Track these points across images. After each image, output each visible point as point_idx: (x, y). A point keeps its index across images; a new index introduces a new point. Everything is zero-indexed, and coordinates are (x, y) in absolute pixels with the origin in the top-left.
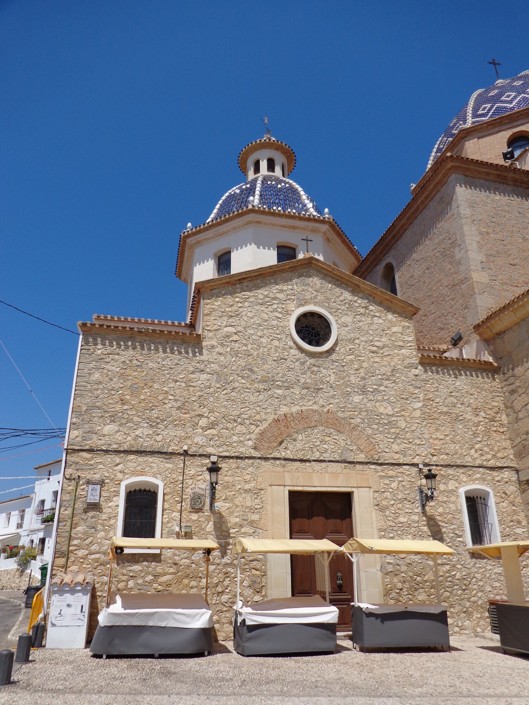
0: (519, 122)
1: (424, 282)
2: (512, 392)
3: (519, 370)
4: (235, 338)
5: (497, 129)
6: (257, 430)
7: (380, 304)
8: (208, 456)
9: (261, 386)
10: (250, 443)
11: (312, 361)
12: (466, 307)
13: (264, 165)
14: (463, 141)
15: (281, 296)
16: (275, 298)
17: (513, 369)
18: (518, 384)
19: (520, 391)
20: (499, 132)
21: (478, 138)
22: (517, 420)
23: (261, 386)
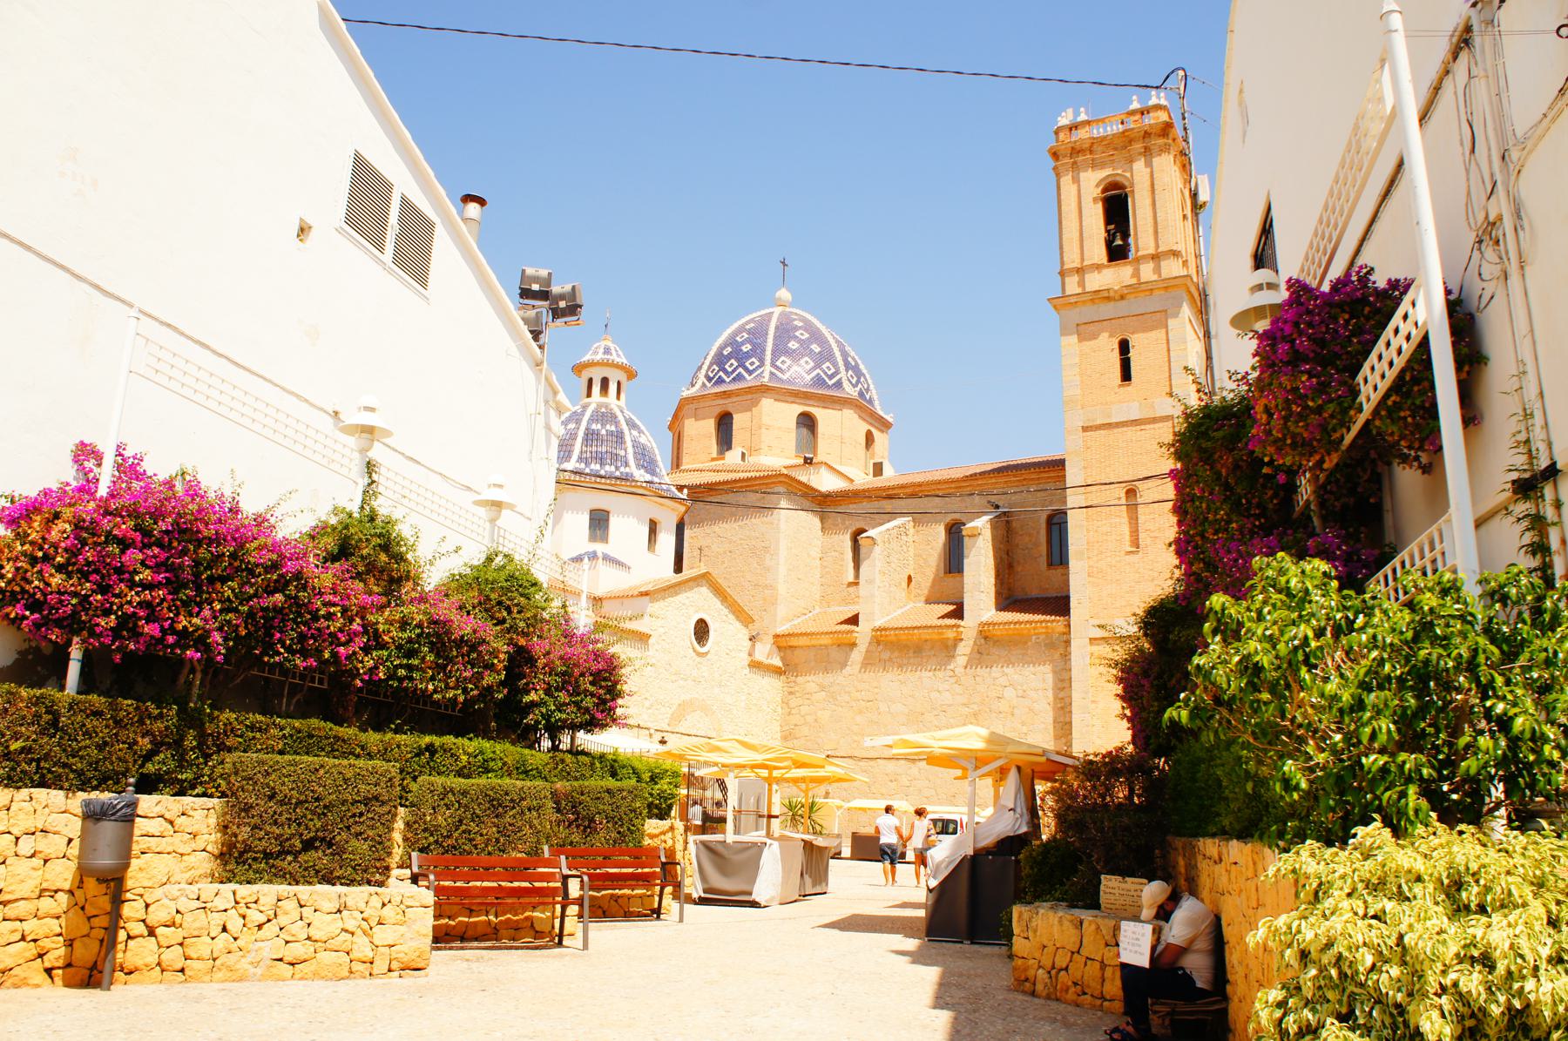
0: (811, 402)
1: (723, 562)
2: (791, 693)
3: (800, 679)
4: (664, 637)
5: (792, 399)
6: (670, 712)
7: (734, 613)
8: (648, 729)
9: (673, 678)
10: (667, 721)
11: (698, 659)
12: (765, 610)
13: (613, 387)
14: (760, 394)
15: (687, 602)
16: (684, 604)
17: (797, 676)
18: (797, 689)
19: (798, 695)
20: (792, 402)
21: (775, 400)
22: (790, 714)
23: (673, 678)
